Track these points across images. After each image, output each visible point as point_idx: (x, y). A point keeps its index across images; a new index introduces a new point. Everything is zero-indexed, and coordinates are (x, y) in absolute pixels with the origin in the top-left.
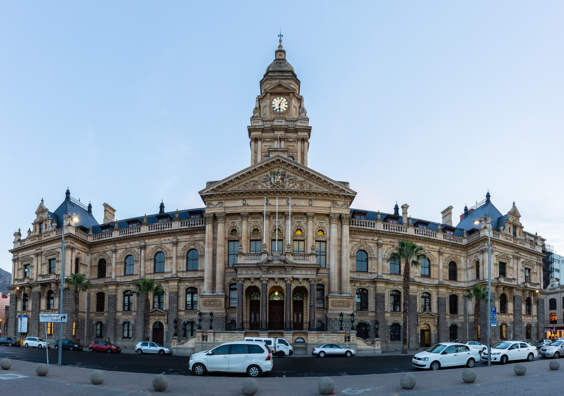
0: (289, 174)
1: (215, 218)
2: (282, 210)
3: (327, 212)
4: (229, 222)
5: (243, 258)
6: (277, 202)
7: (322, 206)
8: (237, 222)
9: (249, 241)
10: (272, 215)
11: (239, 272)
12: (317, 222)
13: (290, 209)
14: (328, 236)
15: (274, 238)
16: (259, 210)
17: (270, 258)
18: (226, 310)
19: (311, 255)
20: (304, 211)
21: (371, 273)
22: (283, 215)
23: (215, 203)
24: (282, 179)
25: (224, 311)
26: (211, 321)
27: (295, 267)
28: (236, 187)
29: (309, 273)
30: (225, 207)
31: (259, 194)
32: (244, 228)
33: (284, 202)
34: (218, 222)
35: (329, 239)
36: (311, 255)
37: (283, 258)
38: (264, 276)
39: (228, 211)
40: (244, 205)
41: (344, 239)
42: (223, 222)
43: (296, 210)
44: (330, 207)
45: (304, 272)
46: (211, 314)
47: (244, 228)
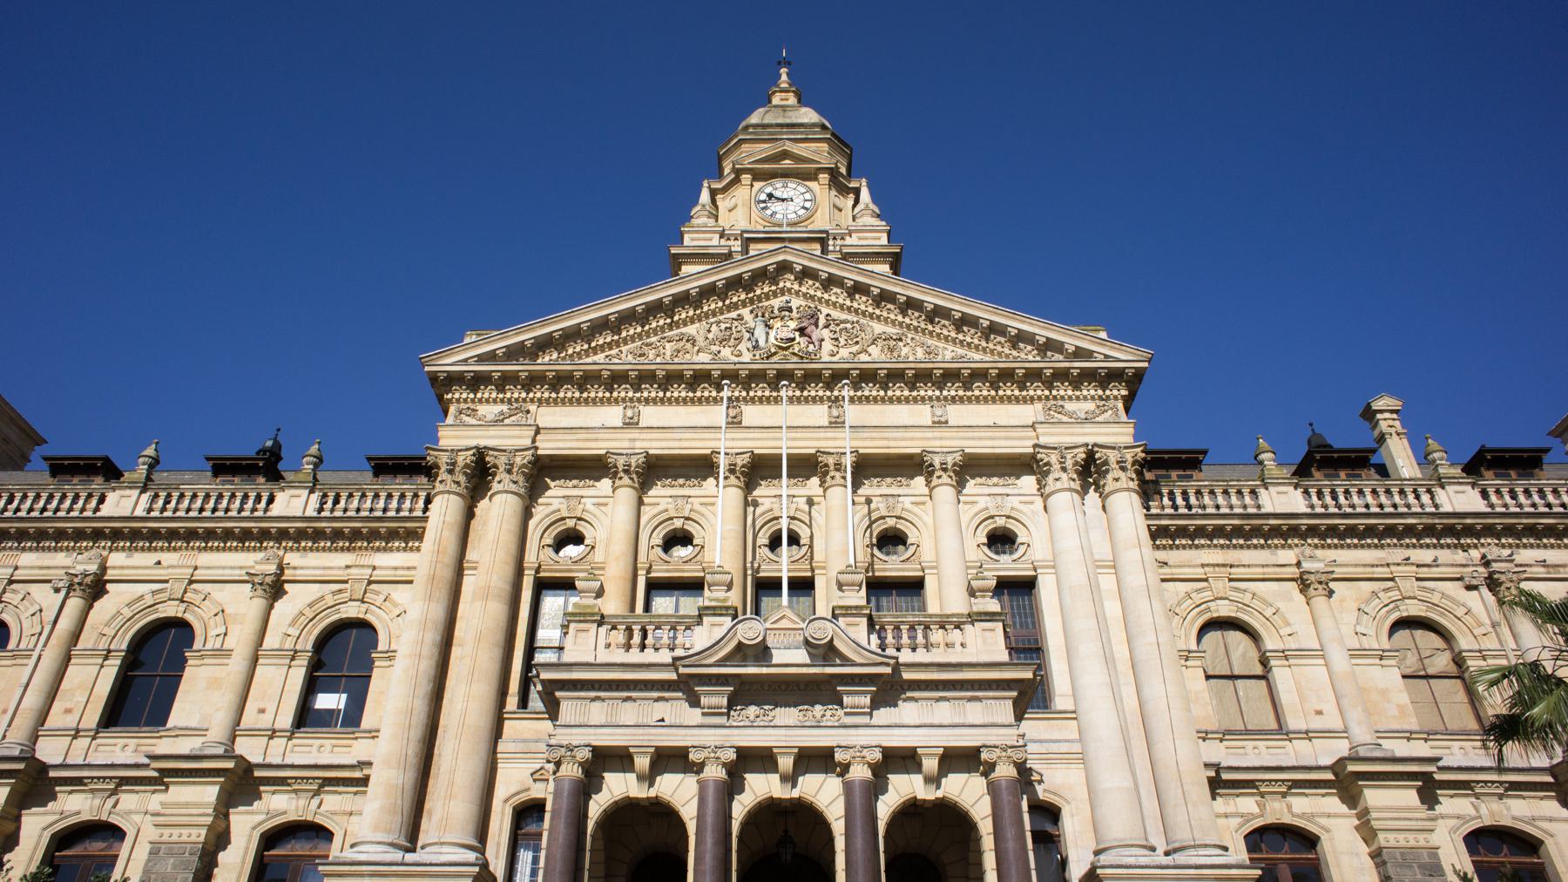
0: (836, 314)
10: (759, 469)
11: (570, 707)
13: (845, 445)
15: (766, 572)
21: (1308, 735)
23: (489, 411)
27: (889, 689)
28: (600, 358)
29: (976, 712)
33: (818, 414)
34: (495, 486)
37: (823, 631)
38: (711, 737)
39: (547, 447)
40: (631, 424)
44: (1033, 426)
45: (944, 711)
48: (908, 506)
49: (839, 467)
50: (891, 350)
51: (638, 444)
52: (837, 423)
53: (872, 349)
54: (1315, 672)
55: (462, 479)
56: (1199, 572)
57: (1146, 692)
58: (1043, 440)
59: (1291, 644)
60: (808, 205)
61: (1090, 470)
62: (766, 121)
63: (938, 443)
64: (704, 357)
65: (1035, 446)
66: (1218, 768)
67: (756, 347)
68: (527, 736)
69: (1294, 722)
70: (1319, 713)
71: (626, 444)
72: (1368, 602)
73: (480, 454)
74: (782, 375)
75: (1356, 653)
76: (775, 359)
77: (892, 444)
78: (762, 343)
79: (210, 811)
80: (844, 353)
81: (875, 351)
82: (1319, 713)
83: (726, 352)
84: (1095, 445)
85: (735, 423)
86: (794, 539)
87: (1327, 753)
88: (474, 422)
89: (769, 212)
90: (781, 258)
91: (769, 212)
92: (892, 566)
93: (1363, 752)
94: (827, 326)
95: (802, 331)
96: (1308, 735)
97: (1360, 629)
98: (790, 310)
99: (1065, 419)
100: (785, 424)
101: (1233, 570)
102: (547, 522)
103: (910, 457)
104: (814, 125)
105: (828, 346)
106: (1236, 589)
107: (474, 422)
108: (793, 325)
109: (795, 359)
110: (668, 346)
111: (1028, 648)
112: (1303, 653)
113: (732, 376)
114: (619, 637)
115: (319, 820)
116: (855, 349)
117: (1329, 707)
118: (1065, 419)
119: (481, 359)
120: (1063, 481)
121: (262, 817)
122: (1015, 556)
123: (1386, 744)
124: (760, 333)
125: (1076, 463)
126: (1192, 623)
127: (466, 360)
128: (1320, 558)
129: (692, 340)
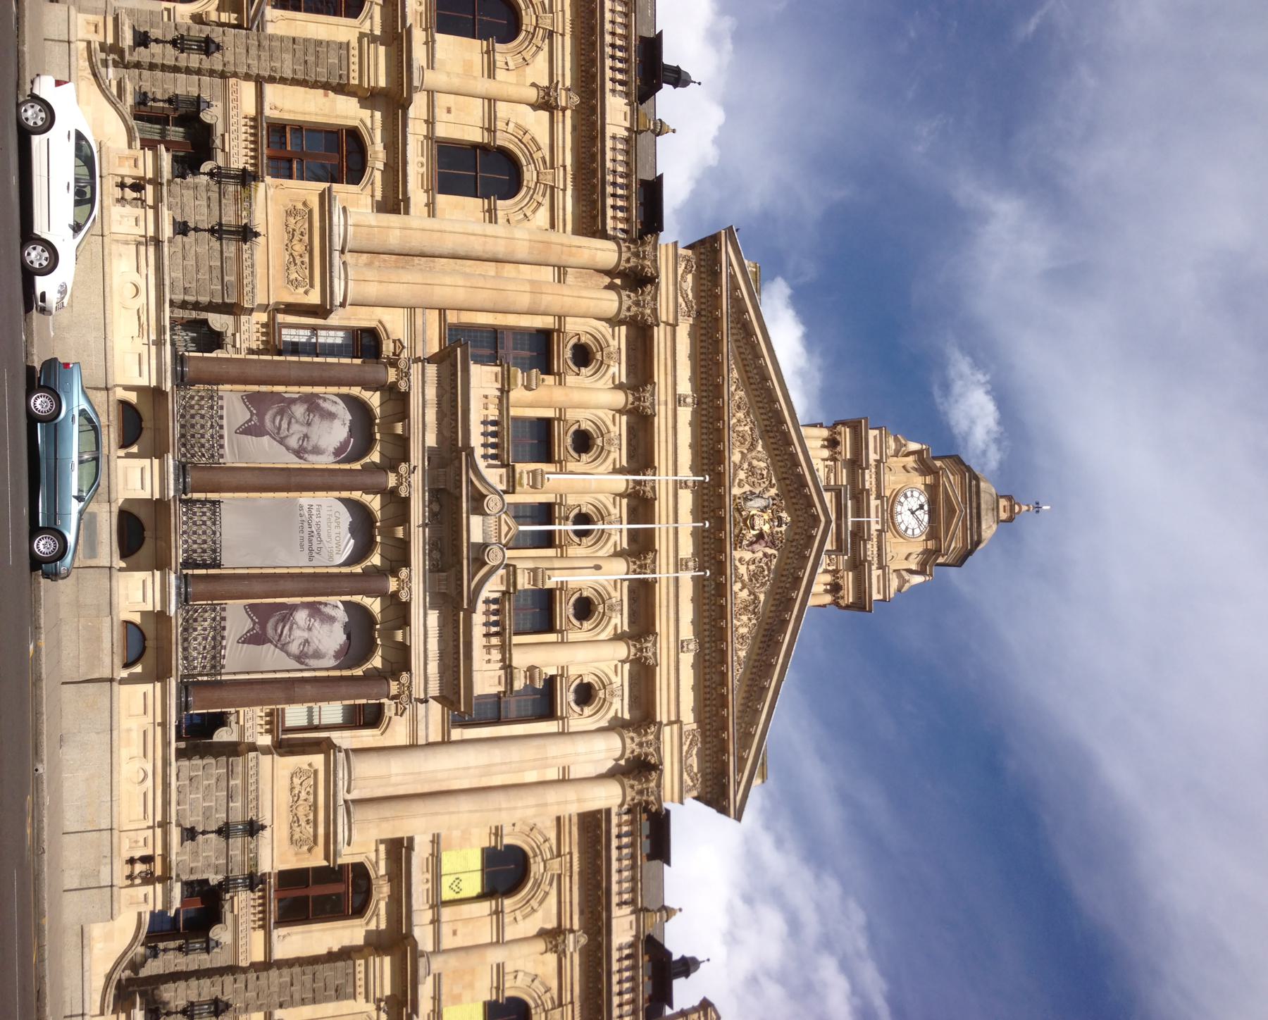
1: (636, 280)
2: (662, 543)
3: (662, 714)
4: (618, 340)
5: (493, 390)
6: (687, 524)
7: (678, 693)
8: (618, 370)
9: (549, 413)
12: (620, 680)
13: (663, 573)
14: (576, 724)
16: (661, 456)
17: (492, 503)
18: (264, 308)
19: (508, 668)
20: (662, 623)
22: (641, 547)
24: (761, 536)
25: (261, 299)
26: (218, 231)
30: (674, 326)
31: (710, 454)
32: (592, 398)
33: (687, 548)
35: (562, 734)
36: (508, 668)
39: (660, 334)
40: (679, 400)
41: (569, 793)
42: (624, 314)
43: (662, 595)
46: (246, 234)
47: (592, 398)
48: (613, 621)
49: (643, 567)
50: (745, 608)
51: (663, 408)
52: (680, 565)
53: (746, 592)
54: (485, 934)
55: (632, 264)
56: (565, 849)
57: (465, 804)
58: (667, 730)
59: (508, 919)
60: (910, 532)
61: (639, 768)
62: (982, 495)
64: (736, 457)
65: (661, 723)
66: (410, 848)
67: (746, 499)
68: (428, 333)
69: (446, 913)
70: (455, 933)
71: (663, 398)
72: (543, 984)
73: (652, 280)
74: (721, 521)
75: (500, 968)
76: (737, 515)
77: (664, 610)
78: (749, 504)
79: (372, 84)
80: (742, 570)
81: (744, 594)
82: (455, 933)
83: (742, 475)
84: (662, 771)
85: (679, 485)
86: (586, 533)
87: (423, 935)
88: (680, 271)
89: (902, 499)
90: (823, 519)
91: (902, 499)
92: (565, 610)
93: (422, 962)
94: (765, 555)
95: (761, 536)
96: (436, 921)
97: (520, 975)
98: (780, 526)
99: (685, 748)
100: (677, 527)
101: (568, 879)
102: (599, 336)
103: (654, 624)
104: (979, 535)
105: (748, 556)
106: (552, 876)
107: (680, 271)
108: (766, 528)
109: (737, 531)
110: (747, 428)
111: (494, 712)
112: (500, 928)
113: (719, 480)
114: (493, 414)
115: (368, 170)
116: (746, 578)
117: (459, 942)
118: (685, 748)
119: (732, 277)
120: (633, 744)
121: (369, 125)
122: (573, 704)
123: (430, 980)
124: (760, 503)
125: (647, 755)
126: (533, 849)
127: (731, 265)
128: (574, 944)
129: (752, 447)
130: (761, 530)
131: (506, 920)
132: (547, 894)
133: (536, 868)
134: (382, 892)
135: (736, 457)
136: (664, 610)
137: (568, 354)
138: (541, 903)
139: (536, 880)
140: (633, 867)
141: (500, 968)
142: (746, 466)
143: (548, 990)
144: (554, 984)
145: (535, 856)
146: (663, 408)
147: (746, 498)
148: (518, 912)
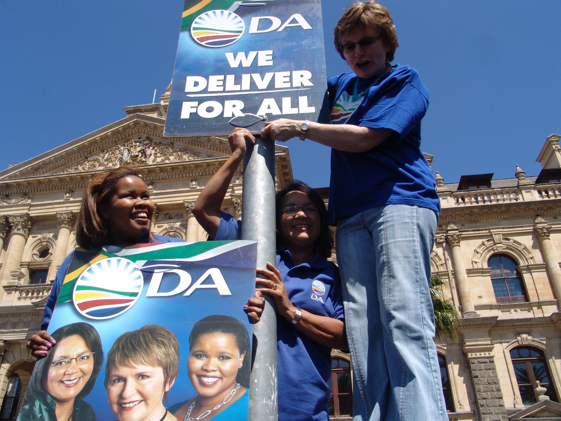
51: (70, 208)
63: (192, 197)
71: (65, 209)
80: (159, 160)
81: (172, 158)
102: (35, 244)
116: (163, 158)
127: (4, 178)
130: (140, 151)
131: (532, 263)
132: (515, 242)
133: (501, 248)
134: (526, 339)
135: (101, 168)
136: (173, 199)
137: (41, 259)
138: (520, 244)
139: (507, 248)
140: (495, 194)
141: (470, 272)
142: (106, 163)
143: (483, 244)
144: (480, 241)
145: (493, 250)
146: (70, 208)
147: (121, 160)
148: (527, 257)
